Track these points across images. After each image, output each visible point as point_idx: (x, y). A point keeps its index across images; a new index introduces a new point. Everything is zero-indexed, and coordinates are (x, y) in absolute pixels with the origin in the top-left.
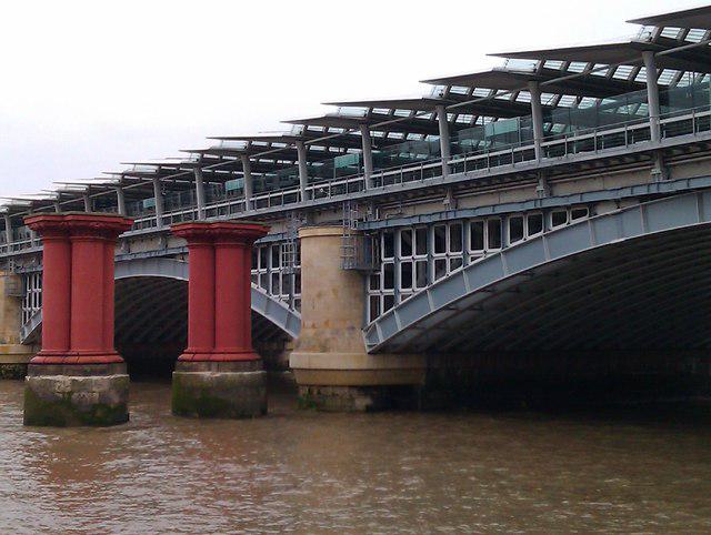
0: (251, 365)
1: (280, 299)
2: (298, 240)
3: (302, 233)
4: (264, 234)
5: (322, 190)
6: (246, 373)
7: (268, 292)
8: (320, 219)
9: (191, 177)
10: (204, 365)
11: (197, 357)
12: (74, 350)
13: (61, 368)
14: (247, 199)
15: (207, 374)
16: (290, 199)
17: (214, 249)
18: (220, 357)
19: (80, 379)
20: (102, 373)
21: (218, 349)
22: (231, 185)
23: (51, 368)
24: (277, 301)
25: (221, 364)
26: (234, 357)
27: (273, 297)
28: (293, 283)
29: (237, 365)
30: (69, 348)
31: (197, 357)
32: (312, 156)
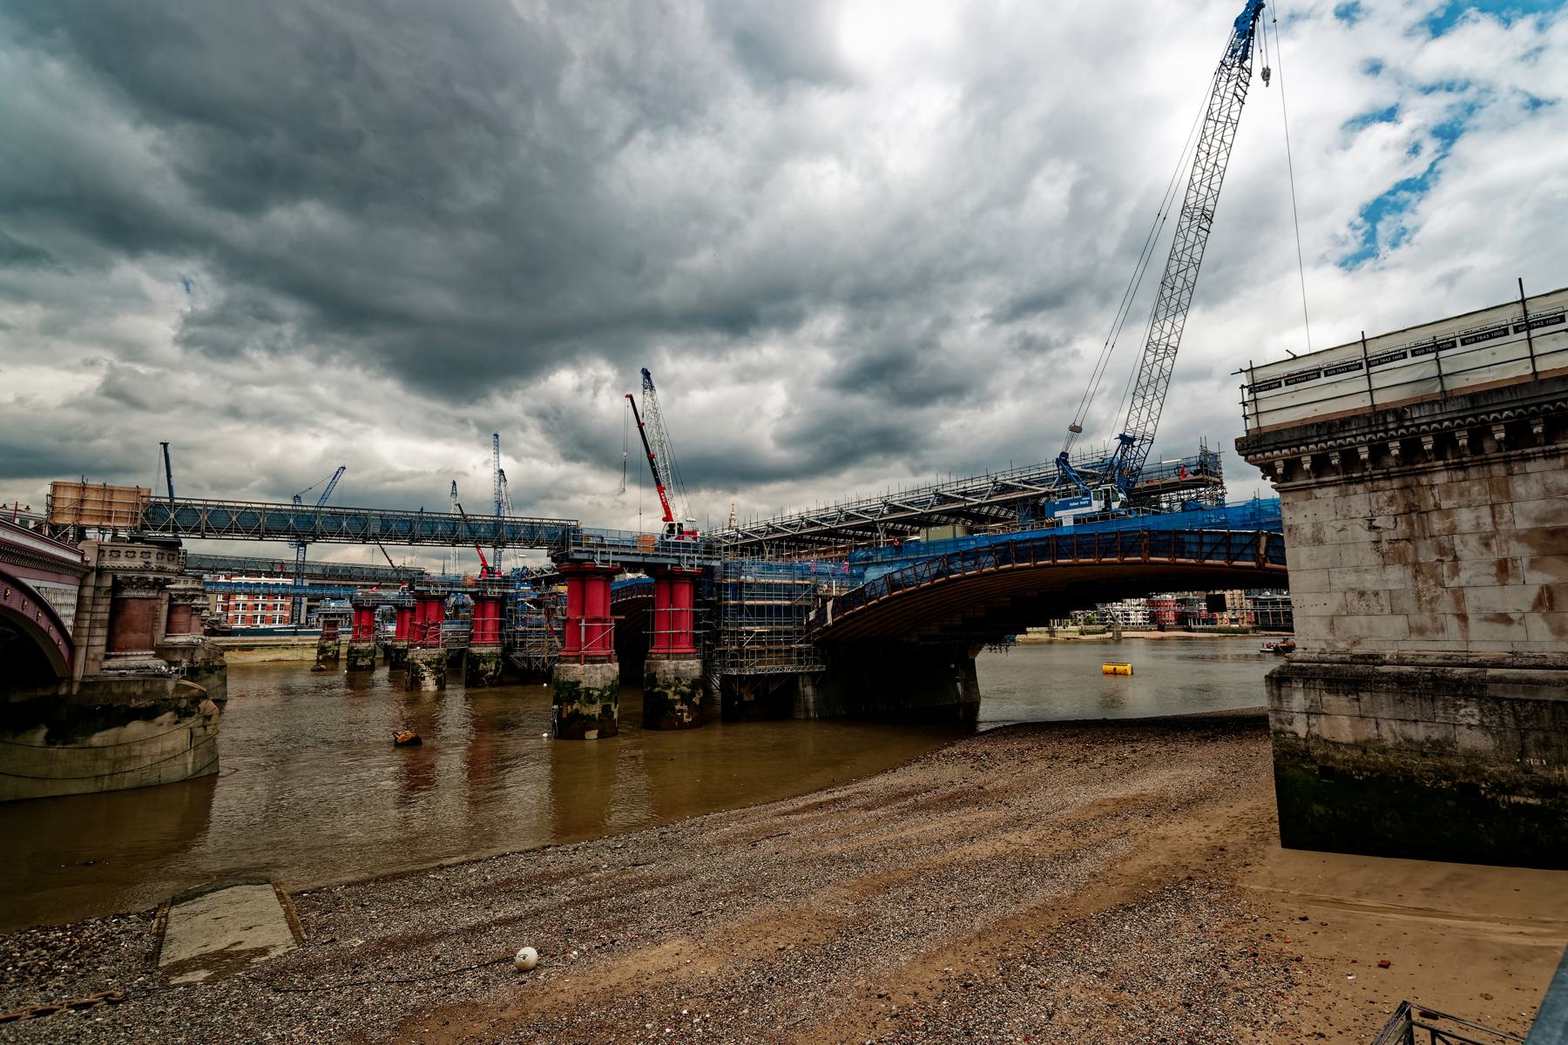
10: (665, 656)
23: (574, 659)
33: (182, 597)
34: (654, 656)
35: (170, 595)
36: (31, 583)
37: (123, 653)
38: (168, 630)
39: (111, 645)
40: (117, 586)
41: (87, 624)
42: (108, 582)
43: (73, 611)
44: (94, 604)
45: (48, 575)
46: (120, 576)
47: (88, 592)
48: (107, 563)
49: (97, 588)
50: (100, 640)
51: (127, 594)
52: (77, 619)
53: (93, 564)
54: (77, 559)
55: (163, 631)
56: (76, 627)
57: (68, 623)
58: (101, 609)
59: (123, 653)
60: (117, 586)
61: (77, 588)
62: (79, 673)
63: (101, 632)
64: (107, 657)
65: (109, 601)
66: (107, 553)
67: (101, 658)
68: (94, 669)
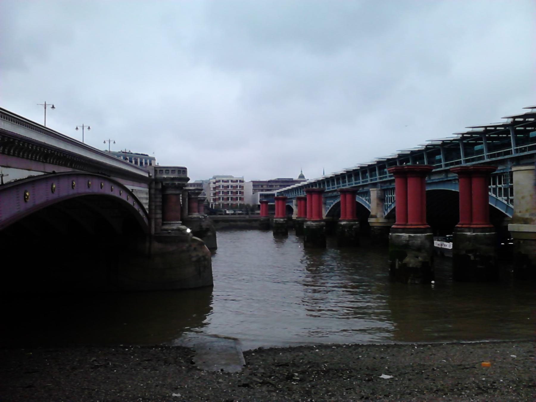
0: (490, 230)
1: (503, 199)
2: (511, 173)
3: (514, 169)
4: (495, 171)
5: (523, 149)
6: (487, 234)
7: (496, 196)
8: (522, 162)
9: (458, 145)
10: (467, 230)
11: (464, 226)
12: (409, 223)
13: (404, 231)
14: (485, 154)
15: (469, 234)
16: (509, 153)
18: (475, 226)
19: (412, 235)
21: (474, 223)
22: (477, 148)
23: (400, 230)
24: (501, 200)
25: (474, 230)
27: (499, 198)
28: (509, 192)
29: (483, 230)
30: (407, 222)
31: (464, 226)
32: (517, 132)
34: (459, 229)
35: (189, 193)
36: (130, 188)
37: (169, 222)
39: (164, 219)
41: (153, 207)
42: (160, 186)
43: (148, 201)
44: (156, 198)
45: (135, 183)
47: (153, 191)
48: (159, 176)
49: (156, 189)
50: (159, 216)
52: (150, 206)
53: (153, 177)
54: (147, 175)
55: (187, 212)
56: (150, 208)
57: (146, 207)
58: (158, 200)
59: (169, 222)
60: (164, 188)
61: (148, 190)
63: (159, 211)
65: (161, 196)
66: (158, 172)
67: (161, 224)
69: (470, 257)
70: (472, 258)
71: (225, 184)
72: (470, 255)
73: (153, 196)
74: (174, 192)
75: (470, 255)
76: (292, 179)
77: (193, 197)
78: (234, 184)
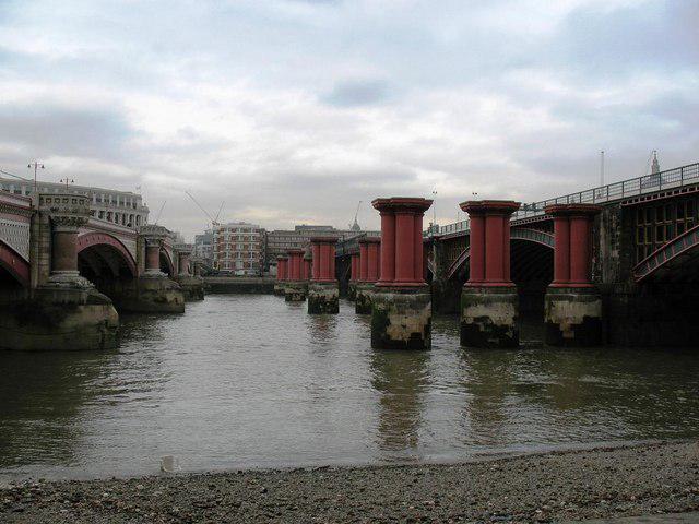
10: (477, 290)
13: (388, 289)
17: (484, 218)
20: (408, 292)
26: (496, 284)
33: (153, 241)
38: (147, 266)
40: (52, 223)
41: (37, 250)
42: (47, 221)
44: (41, 236)
46: (52, 216)
47: (36, 228)
51: (60, 229)
53: (36, 208)
54: (28, 205)
55: (143, 267)
60: (52, 223)
62: (35, 283)
63: (46, 256)
64: (51, 274)
65: (48, 234)
67: (46, 274)
68: (44, 282)
69: (478, 326)
70: (482, 329)
71: (234, 234)
72: (480, 324)
73: (37, 234)
74: (68, 229)
75: (480, 324)
76: (331, 227)
77: (152, 245)
78: (246, 234)
